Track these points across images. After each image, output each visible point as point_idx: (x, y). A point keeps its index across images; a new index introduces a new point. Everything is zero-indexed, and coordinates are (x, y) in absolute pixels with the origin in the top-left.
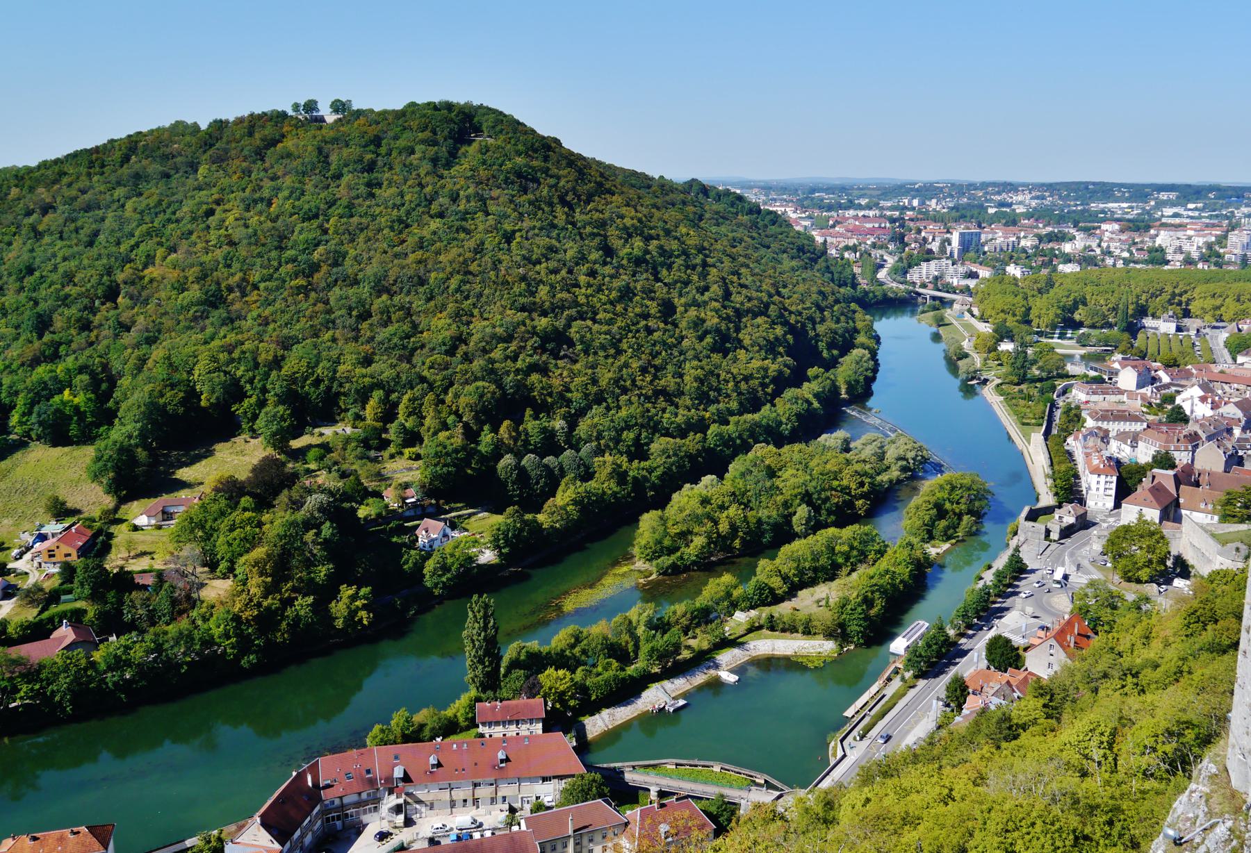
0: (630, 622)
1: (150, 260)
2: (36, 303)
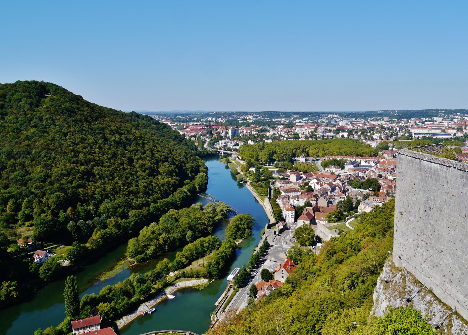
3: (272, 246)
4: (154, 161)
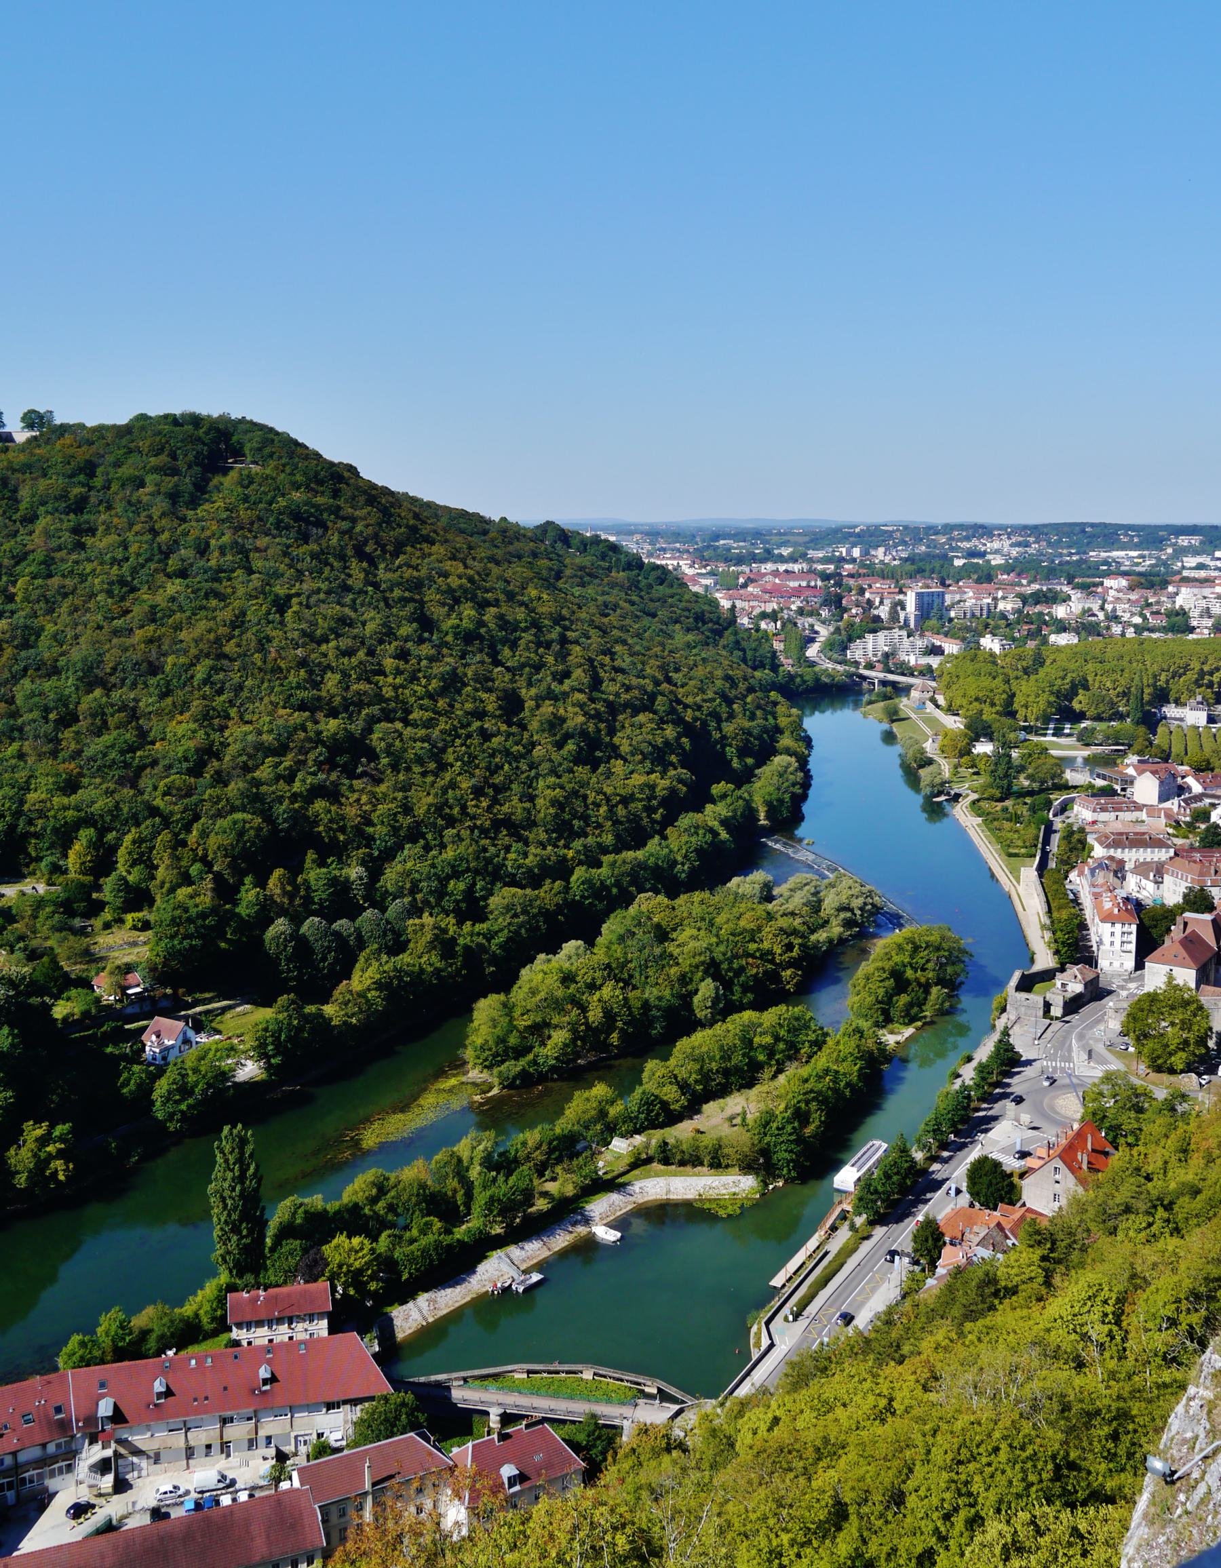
0: (460, 1160)
3: (1029, 1063)
4: (600, 706)
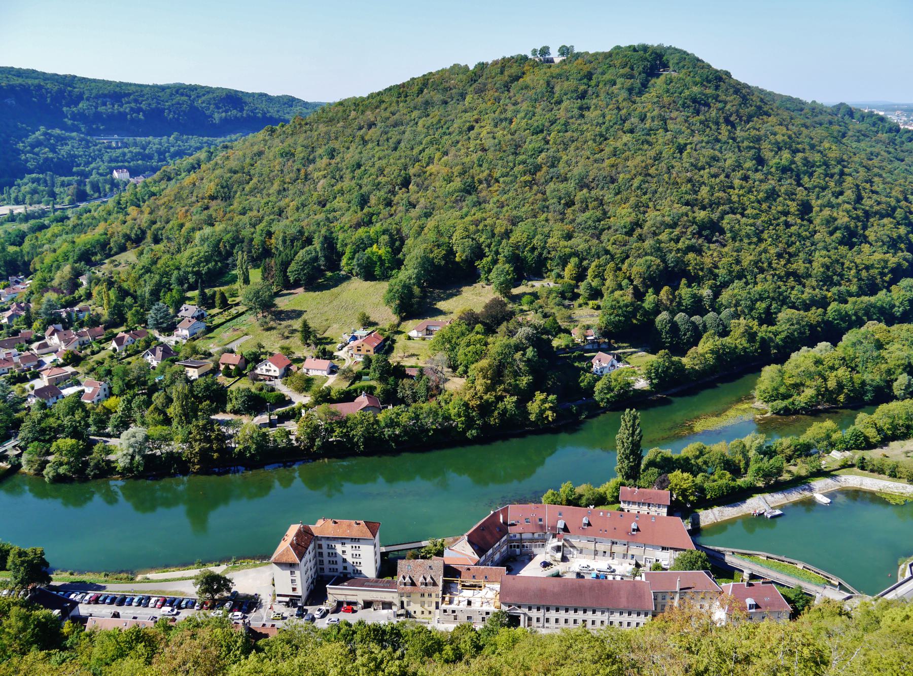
0: (744, 446)
1: (431, 160)
2: (361, 187)
4: (860, 213)
